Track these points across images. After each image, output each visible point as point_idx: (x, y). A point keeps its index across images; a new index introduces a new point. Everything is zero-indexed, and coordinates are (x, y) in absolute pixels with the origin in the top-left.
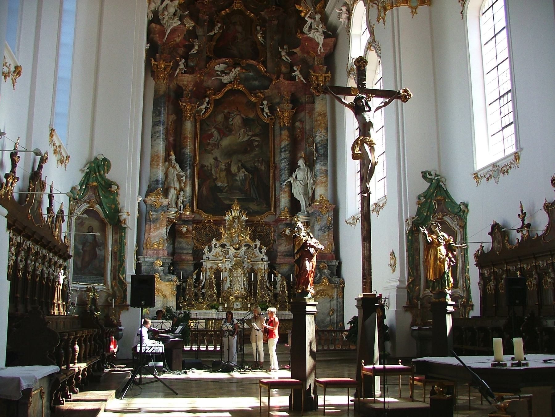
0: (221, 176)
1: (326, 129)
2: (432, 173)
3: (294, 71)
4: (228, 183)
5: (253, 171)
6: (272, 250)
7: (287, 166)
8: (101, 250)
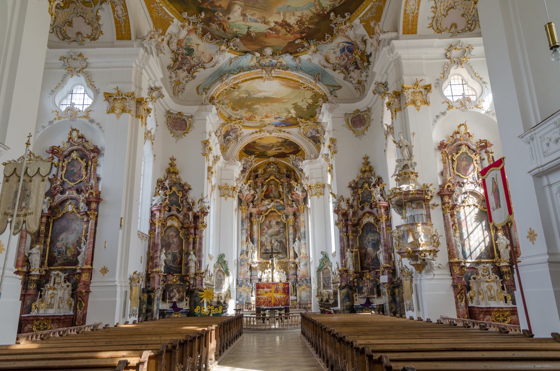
1: (305, 227)
5: (281, 242)
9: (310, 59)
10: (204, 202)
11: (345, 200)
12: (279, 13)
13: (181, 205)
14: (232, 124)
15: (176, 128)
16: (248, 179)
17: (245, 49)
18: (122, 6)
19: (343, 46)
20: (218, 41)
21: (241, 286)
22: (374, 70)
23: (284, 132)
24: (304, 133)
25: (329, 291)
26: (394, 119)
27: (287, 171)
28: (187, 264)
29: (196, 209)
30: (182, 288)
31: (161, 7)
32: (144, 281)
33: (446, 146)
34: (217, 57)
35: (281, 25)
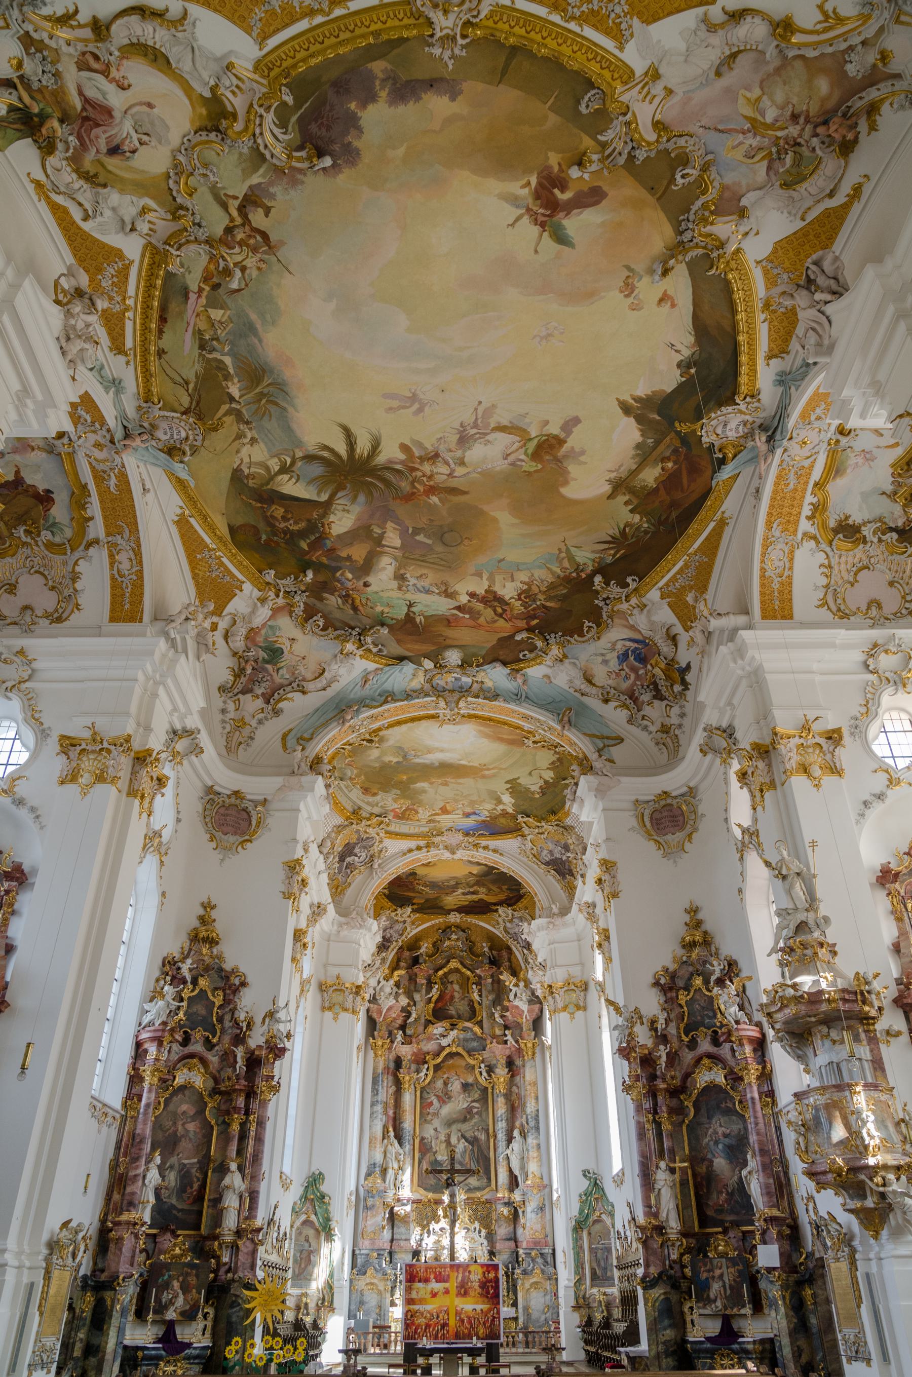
1: (537, 1098)
3: (506, 1035)
5: (473, 1142)
9: (548, 677)
10: (278, 1021)
11: (645, 1020)
12: (479, 574)
13: (218, 1027)
14: (361, 827)
15: (225, 829)
16: (395, 967)
17: (399, 651)
18: (131, 552)
19: (624, 649)
20: (339, 632)
21: (365, 1274)
22: (701, 698)
23: (486, 848)
24: (535, 852)
25: (609, 1290)
26: (759, 809)
27: (491, 949)
28: (217, 1200)
29: (256, 1039)
30: (197, 1276)
31: (219, 558)
32: (89, 1253)
33: (897, 875)
34: (333, 669)
35: (484, 600)
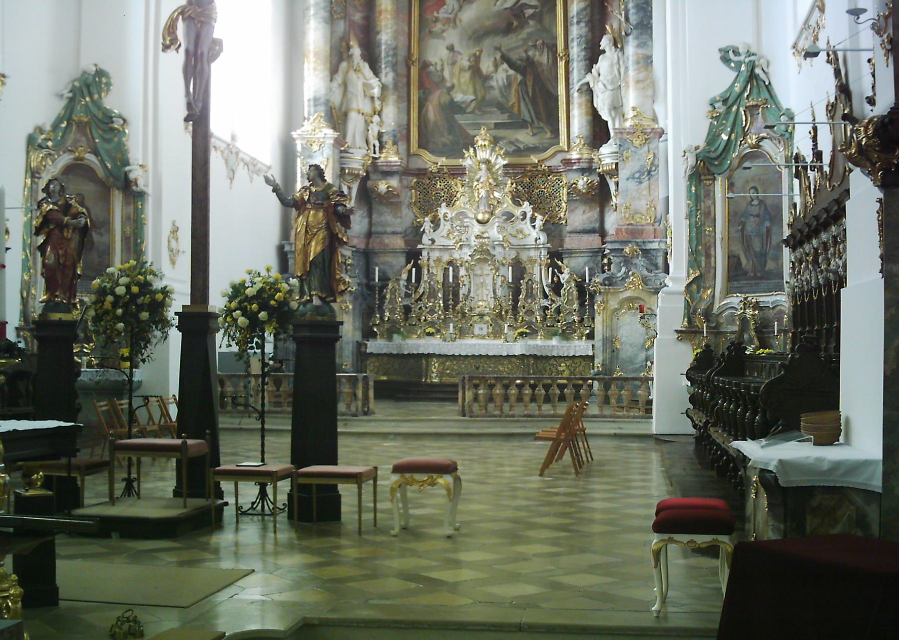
0: (462, 80)
2: (741, 51)
4: (475, 93)
6: (564, 222)
7: (583, 53)
8: (101, 235)
25: (767, 299)
